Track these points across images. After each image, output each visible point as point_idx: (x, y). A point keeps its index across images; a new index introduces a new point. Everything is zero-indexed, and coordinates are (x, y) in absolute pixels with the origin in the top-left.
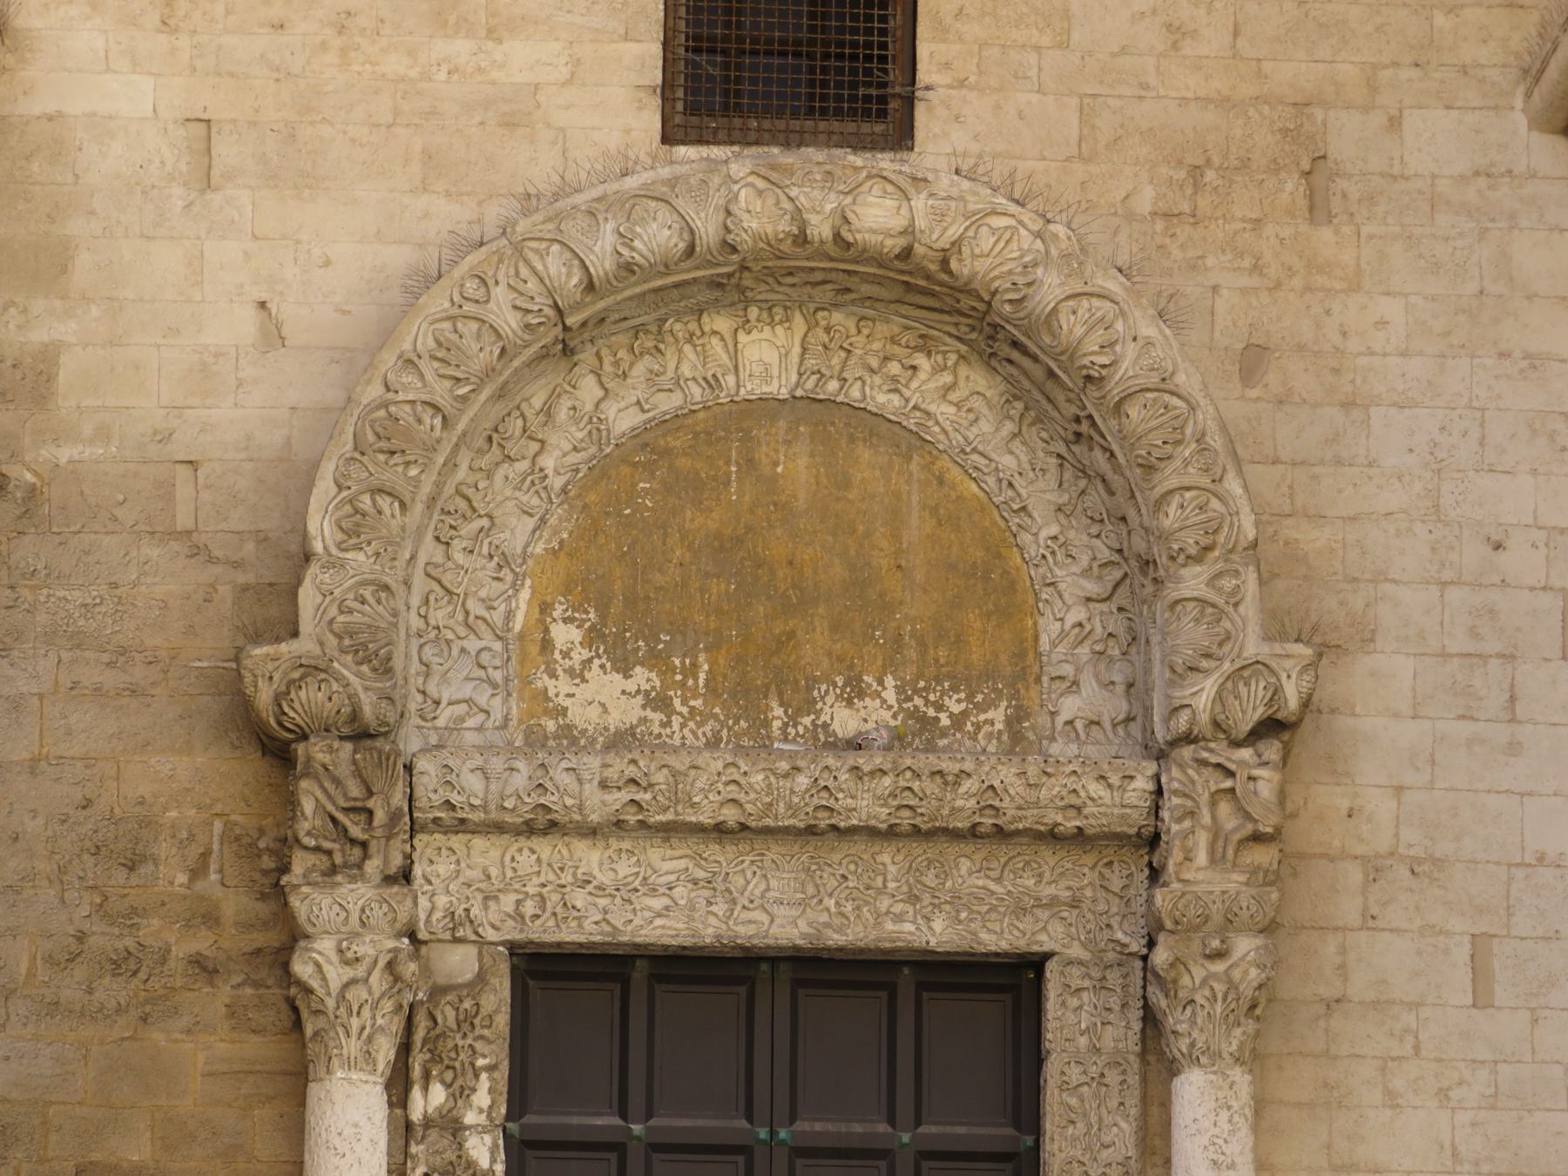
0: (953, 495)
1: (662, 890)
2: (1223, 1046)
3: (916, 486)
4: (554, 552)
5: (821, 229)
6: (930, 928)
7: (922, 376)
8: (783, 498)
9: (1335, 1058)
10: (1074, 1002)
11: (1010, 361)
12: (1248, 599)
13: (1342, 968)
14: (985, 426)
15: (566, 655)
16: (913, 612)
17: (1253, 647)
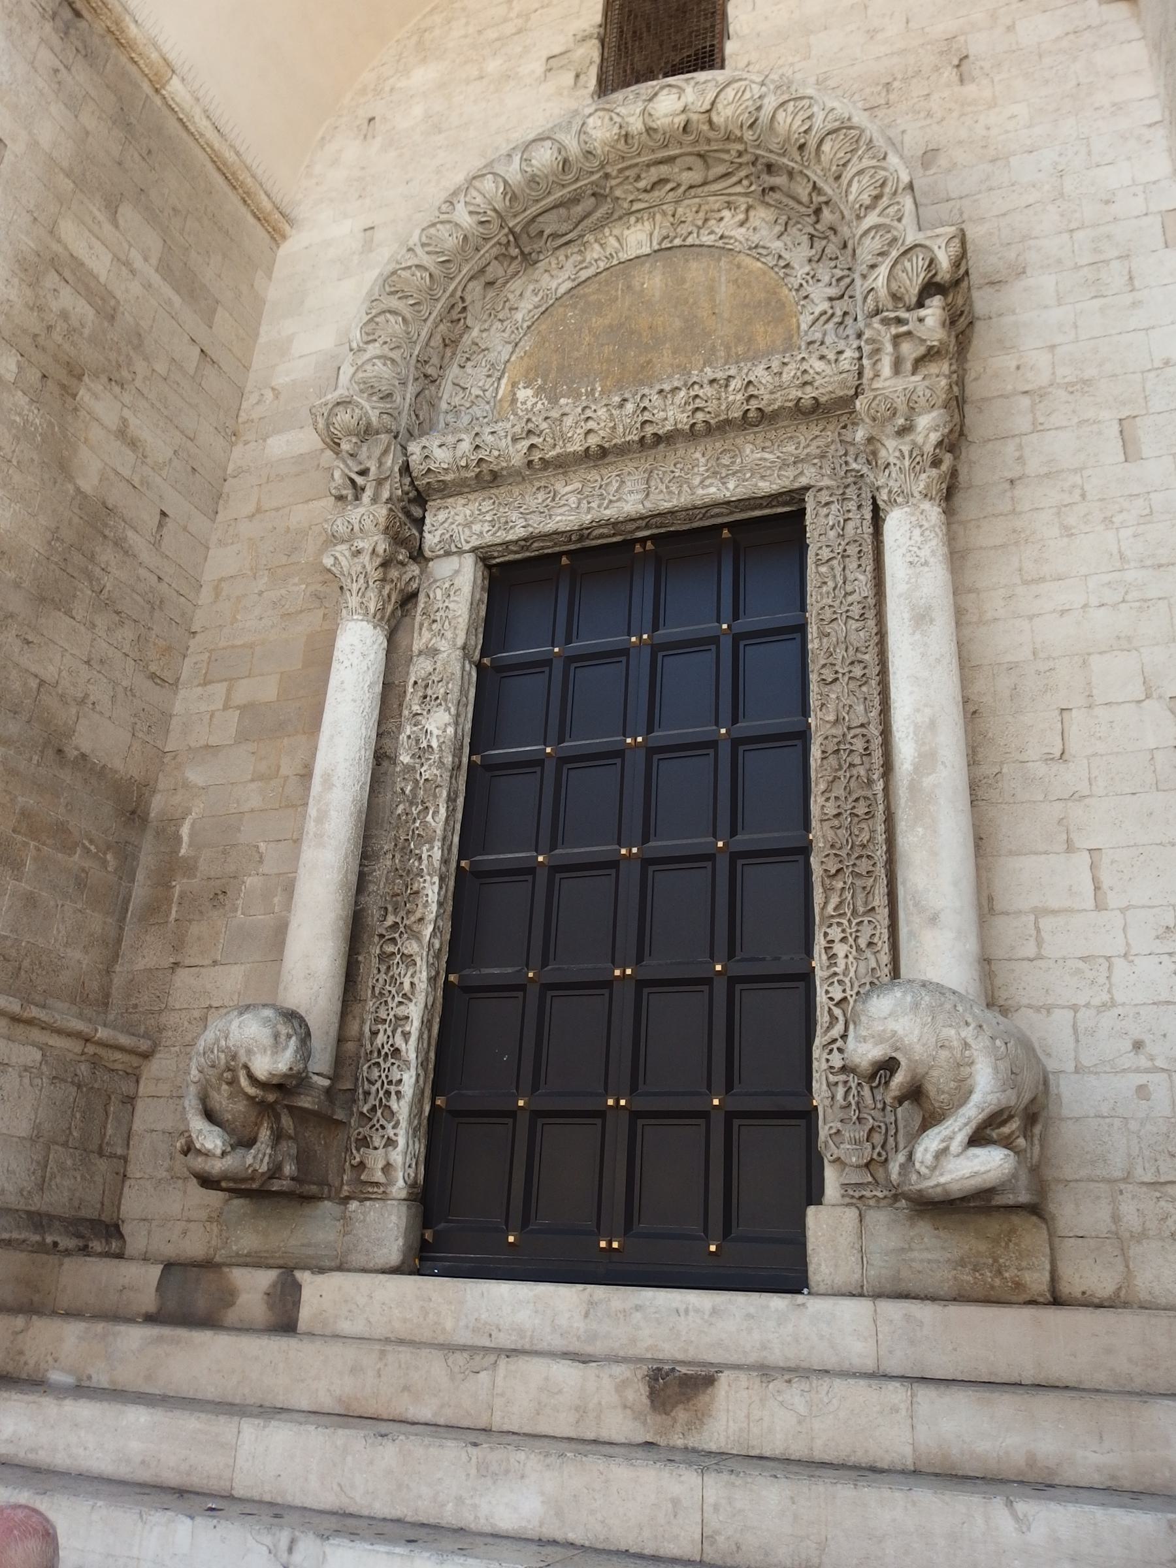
1: (563, 502)
2: (914, 488)
4: (522, 358)
5: (636, 125)
6: (727, 489)
7: (726, 220)
9: (1020, 513)
10: (825, 511)
11: (772, 189)
12: (906, 214)
13: (1020, 459)
14: (764, 232)
15: (524, 403)
16: (722, 334)
17: (912, 237)
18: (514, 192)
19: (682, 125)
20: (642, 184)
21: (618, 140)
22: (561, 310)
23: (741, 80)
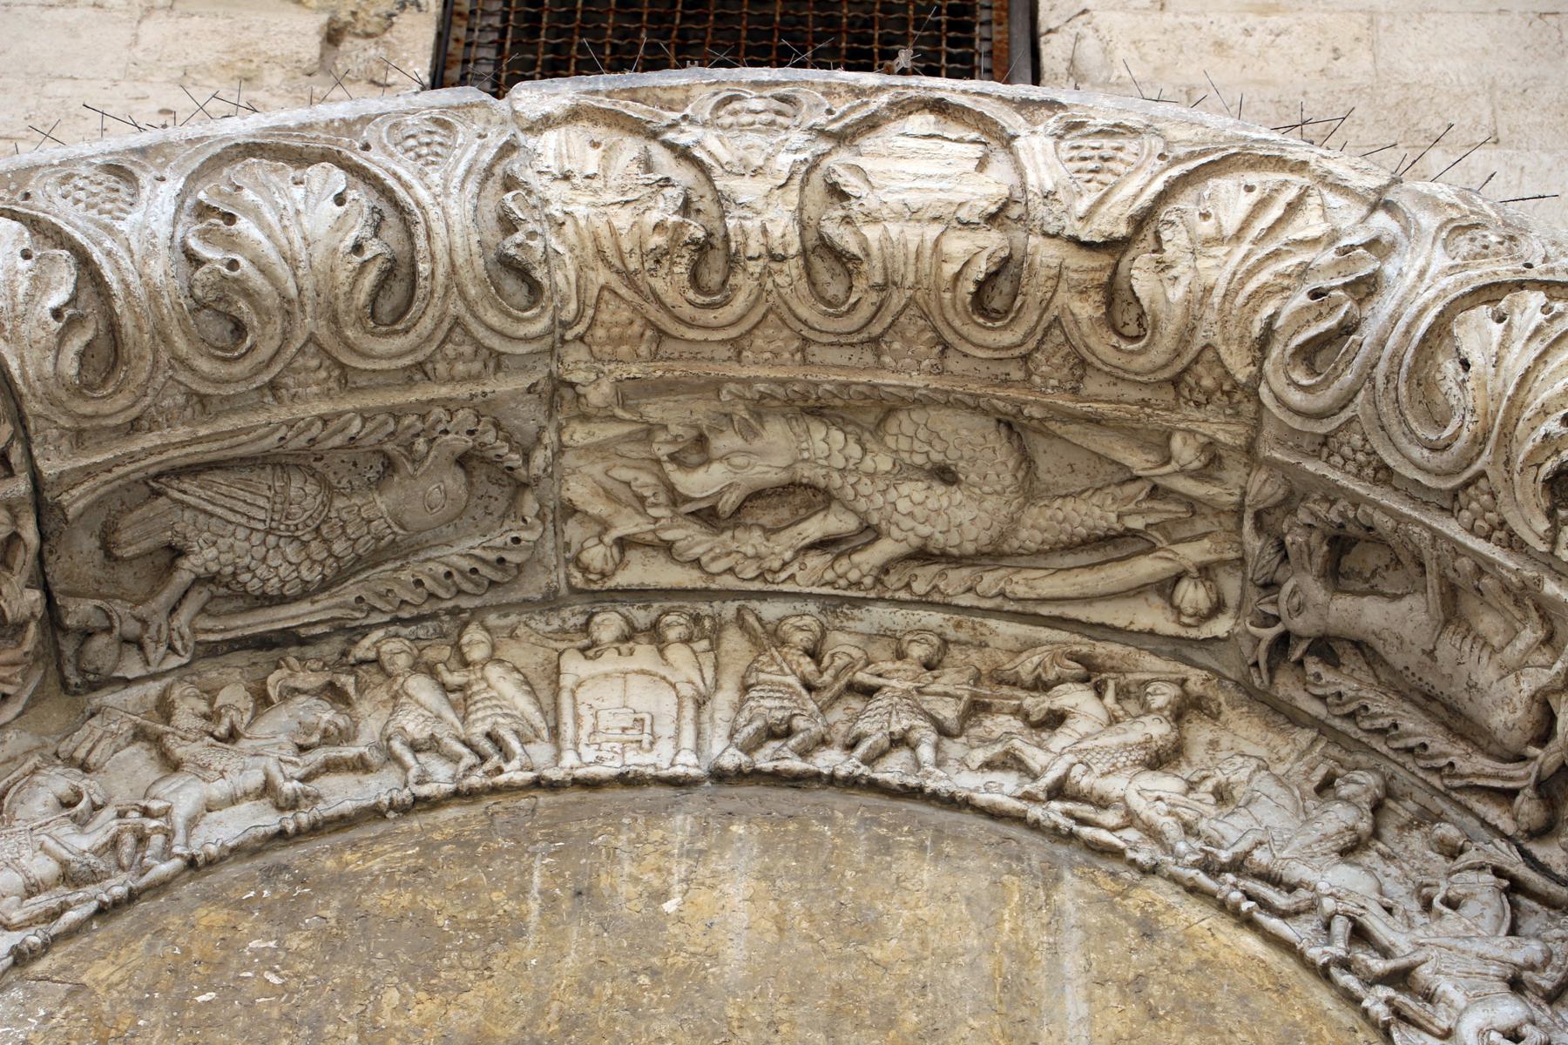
0: (1189, 959)
3: (1078, 935)
8: (680, 960)
11: (1326, 647)
18: (113, 328)
19: (981, 268)
20: (699, 483)
21: (659, 256)
22: (214, 916)
23: (1280, 163)
